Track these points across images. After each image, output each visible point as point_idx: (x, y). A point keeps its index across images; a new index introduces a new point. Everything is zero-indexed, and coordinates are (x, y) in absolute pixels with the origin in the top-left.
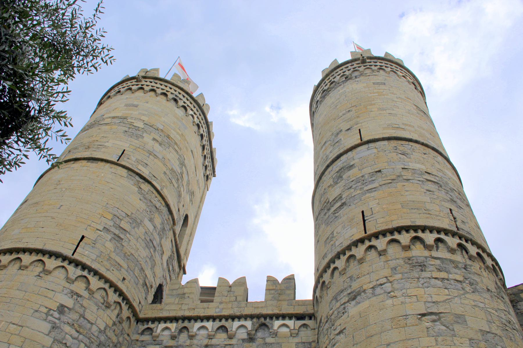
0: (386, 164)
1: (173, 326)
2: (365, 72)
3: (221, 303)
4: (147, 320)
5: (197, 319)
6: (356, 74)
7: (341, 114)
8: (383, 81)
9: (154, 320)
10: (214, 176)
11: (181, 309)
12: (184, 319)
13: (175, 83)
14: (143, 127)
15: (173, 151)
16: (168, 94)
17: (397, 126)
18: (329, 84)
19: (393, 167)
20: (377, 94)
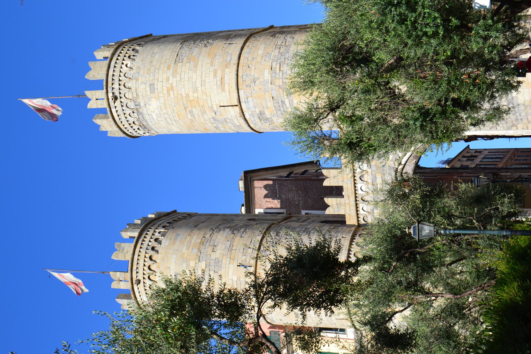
0: (266, 93)
1: (361, 206)
2: (131, 97)
3: (343, 181)
4: (358, 221)
5: (356, 194)
6: (131, 105)
7: (190, 117)
8: (148, 85)
9: (358, 218)
10: (175, 211)
11: (349, 204)
12: (356, 200)
13: (131, 252)
14: (204, 263)
15: (214, 237)
16: (148, 256)
17: (219, 82)
18: (132, 125)
19: (270, 89)
20: (171, 92)
